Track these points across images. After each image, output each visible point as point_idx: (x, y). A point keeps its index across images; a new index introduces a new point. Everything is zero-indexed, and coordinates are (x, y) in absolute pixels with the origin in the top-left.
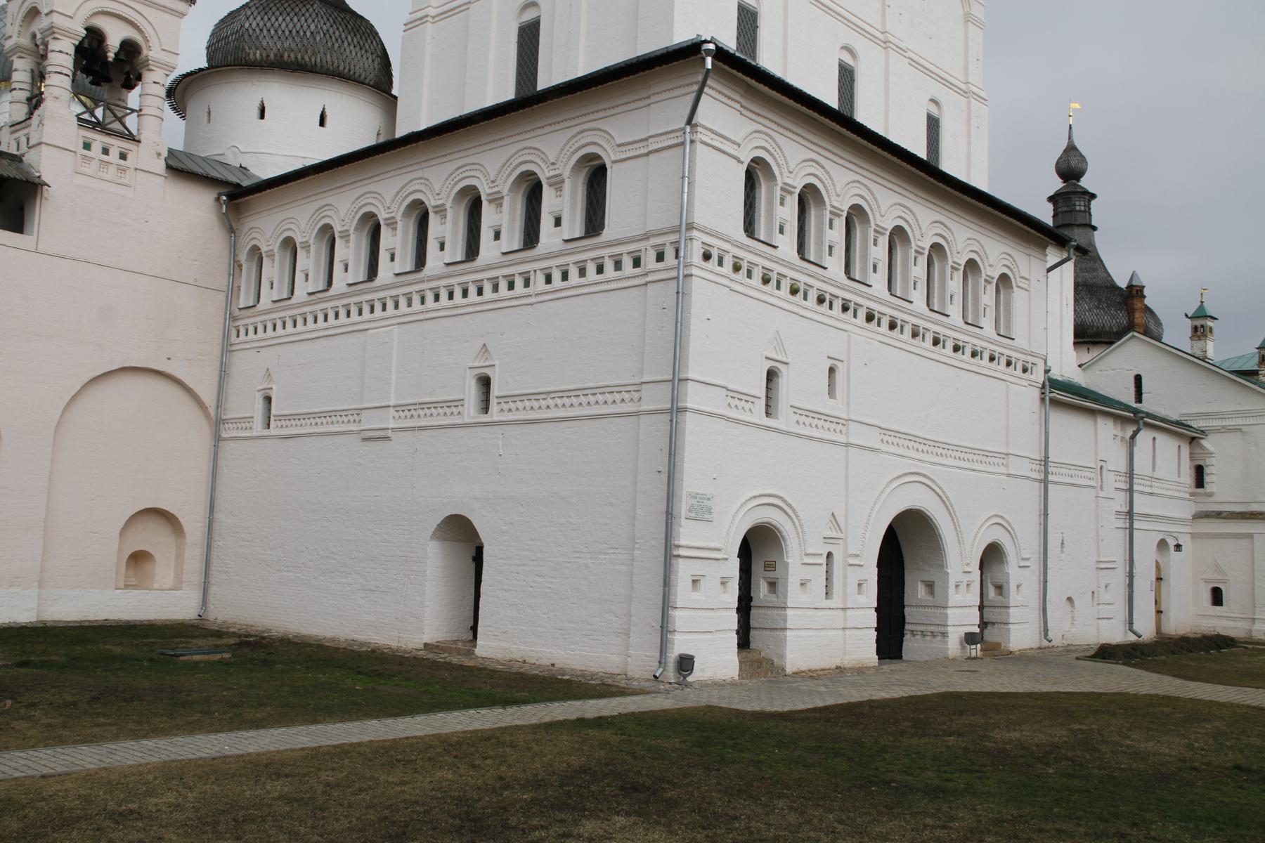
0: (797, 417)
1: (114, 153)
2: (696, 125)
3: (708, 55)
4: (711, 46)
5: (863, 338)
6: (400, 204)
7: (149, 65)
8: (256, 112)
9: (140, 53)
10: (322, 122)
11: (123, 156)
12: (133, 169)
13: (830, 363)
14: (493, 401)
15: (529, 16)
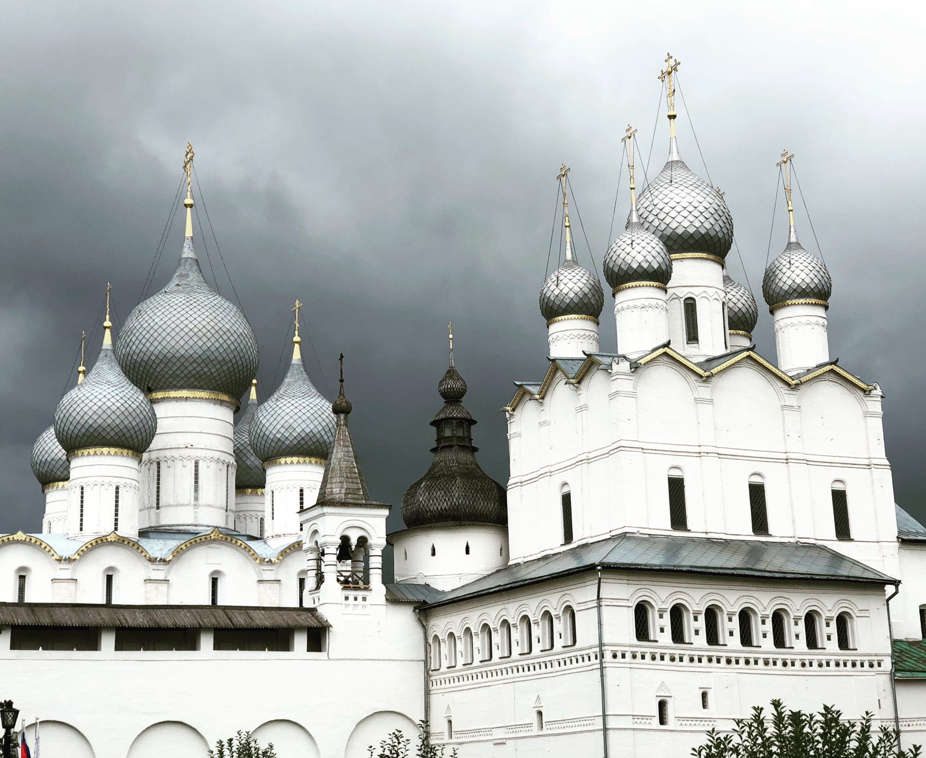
0: (680, 722)
1: (360, 598)
2: (601, 599)
3: (599, 571)
4: (599, 568)
5: (725, 674)
6: (498, 621)
7: (371, 547)
8: (430, 552)
9: (367, 542)
10: (467, 552)
11: (364, 599)
12: (369, 605)
13: (702, 691)
14: (544, 724)
15: (565, 490)
